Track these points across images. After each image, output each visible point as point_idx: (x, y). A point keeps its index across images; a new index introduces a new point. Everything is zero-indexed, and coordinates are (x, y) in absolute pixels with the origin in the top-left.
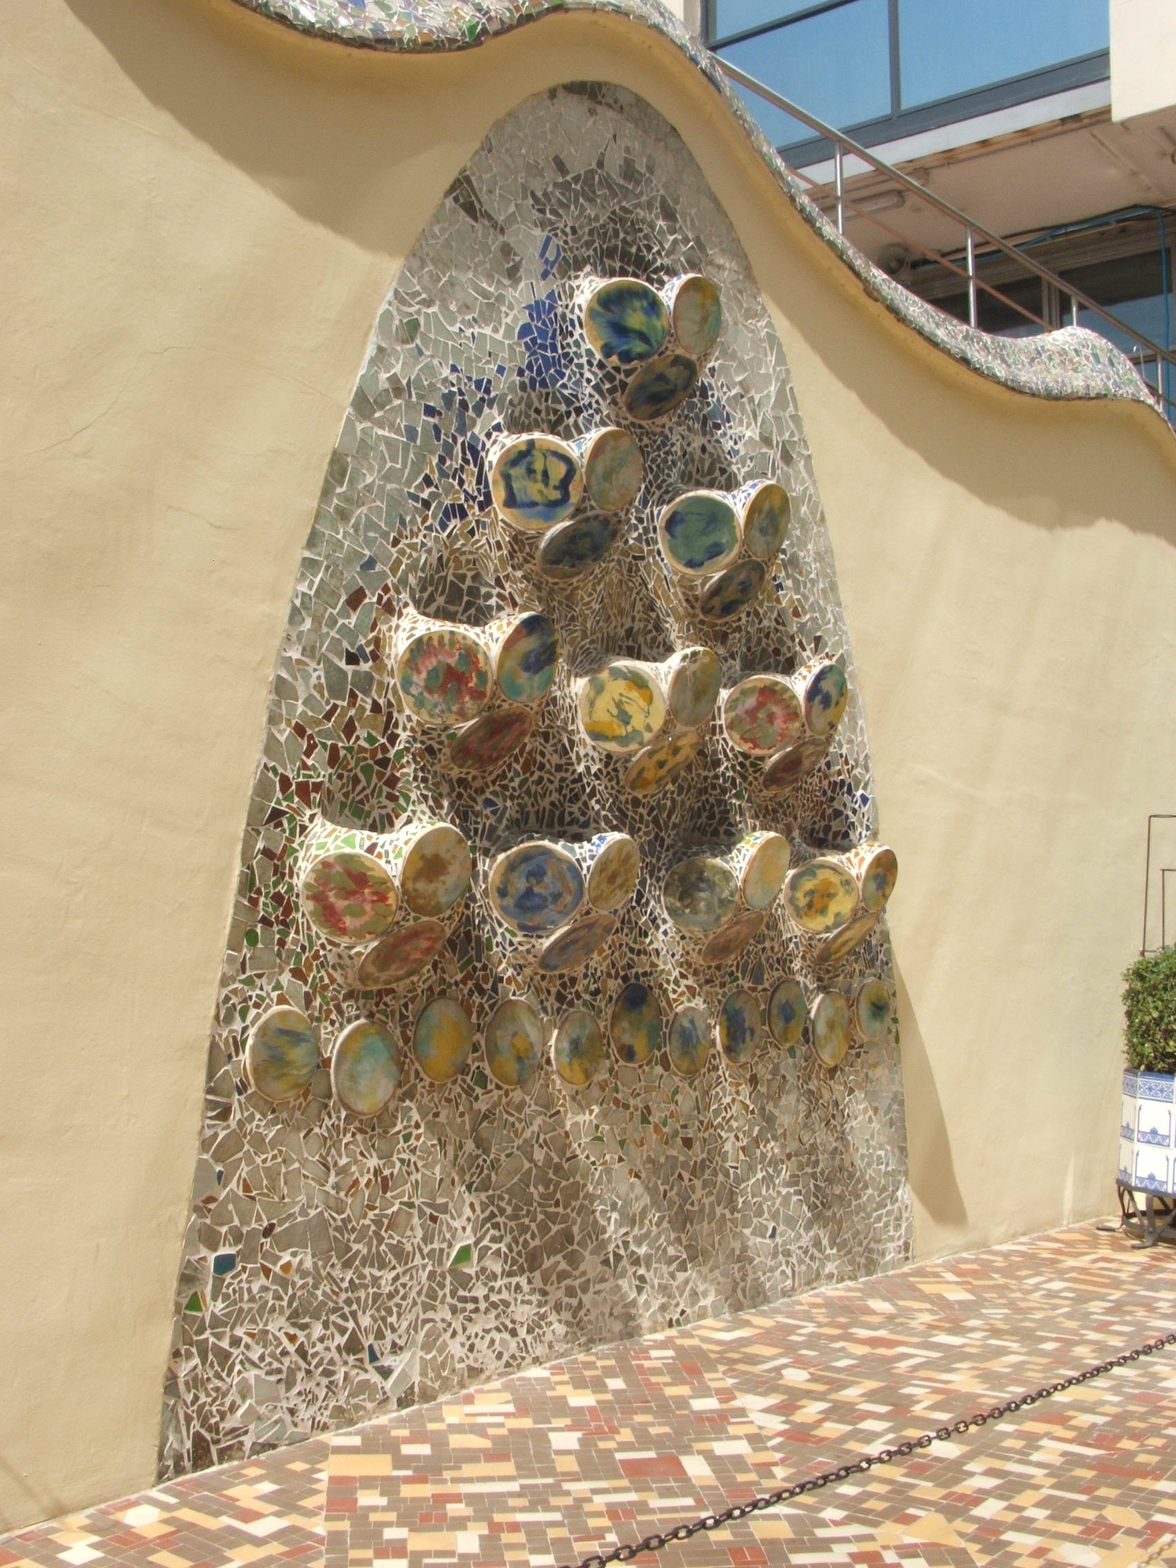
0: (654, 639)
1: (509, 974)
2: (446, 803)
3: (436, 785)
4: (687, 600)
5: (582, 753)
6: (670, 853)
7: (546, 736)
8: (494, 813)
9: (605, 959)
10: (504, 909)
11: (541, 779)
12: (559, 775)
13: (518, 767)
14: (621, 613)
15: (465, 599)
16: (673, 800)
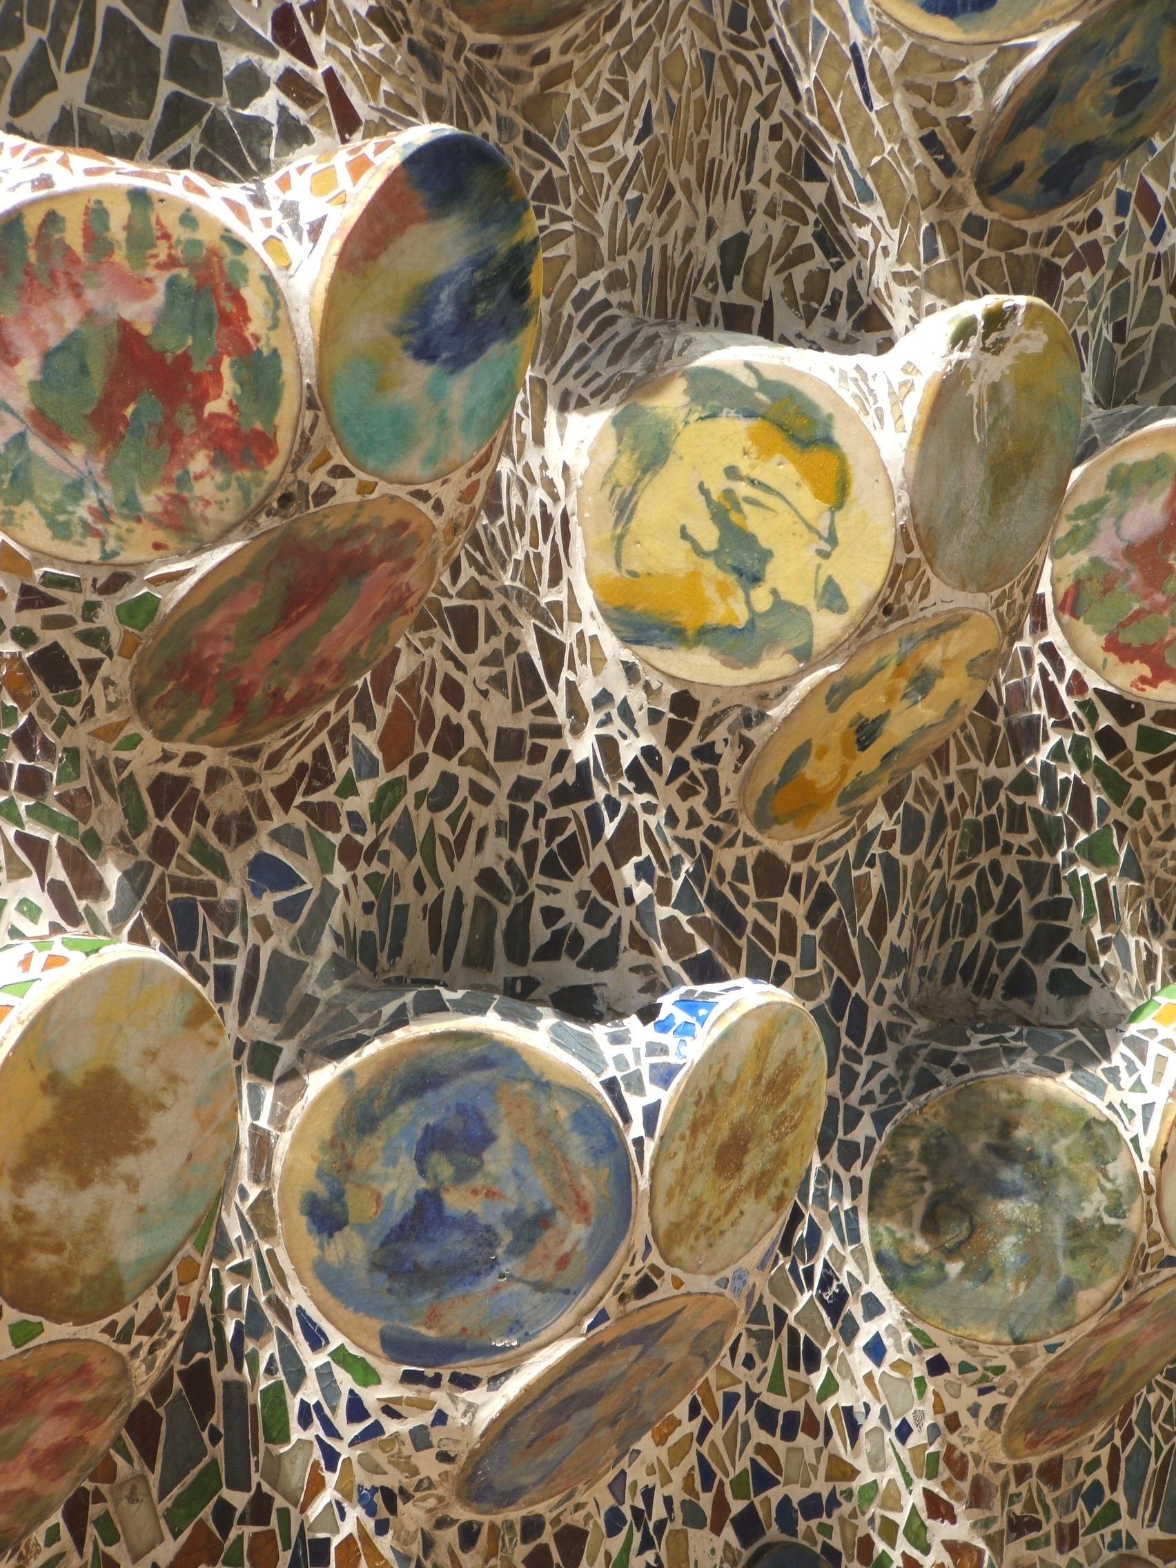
0: (818, 281)
1: (348, 1527)
2: (112, 875)
3: (78, 802)
4: (930, 142)
5: (588, 691)
6: (888, 1058)
7: (464, 626)
8: (287, 910)
9: (677, 1454)
10: (331, 1280)
11: (448, 783)
12: (510, 773)
13: (370, 740)
14: (708, 179)
16: (891, 868)
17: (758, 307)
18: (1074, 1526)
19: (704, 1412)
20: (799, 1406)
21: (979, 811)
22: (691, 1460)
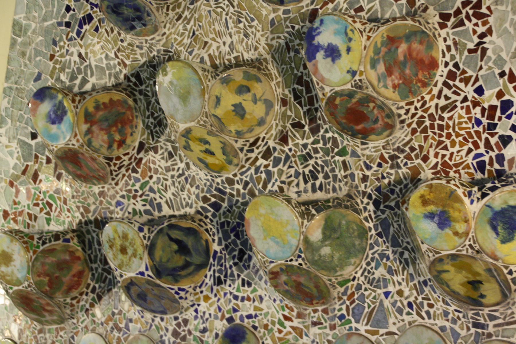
8: (121, 210)
11: (159, 179)
13: (138, 176)
15: (107, 72)
17: (240, 54)
18: (335, 325)
19: (218, 296)
20: (245, 295)
21: (302, 151)
22: (215, 306)
